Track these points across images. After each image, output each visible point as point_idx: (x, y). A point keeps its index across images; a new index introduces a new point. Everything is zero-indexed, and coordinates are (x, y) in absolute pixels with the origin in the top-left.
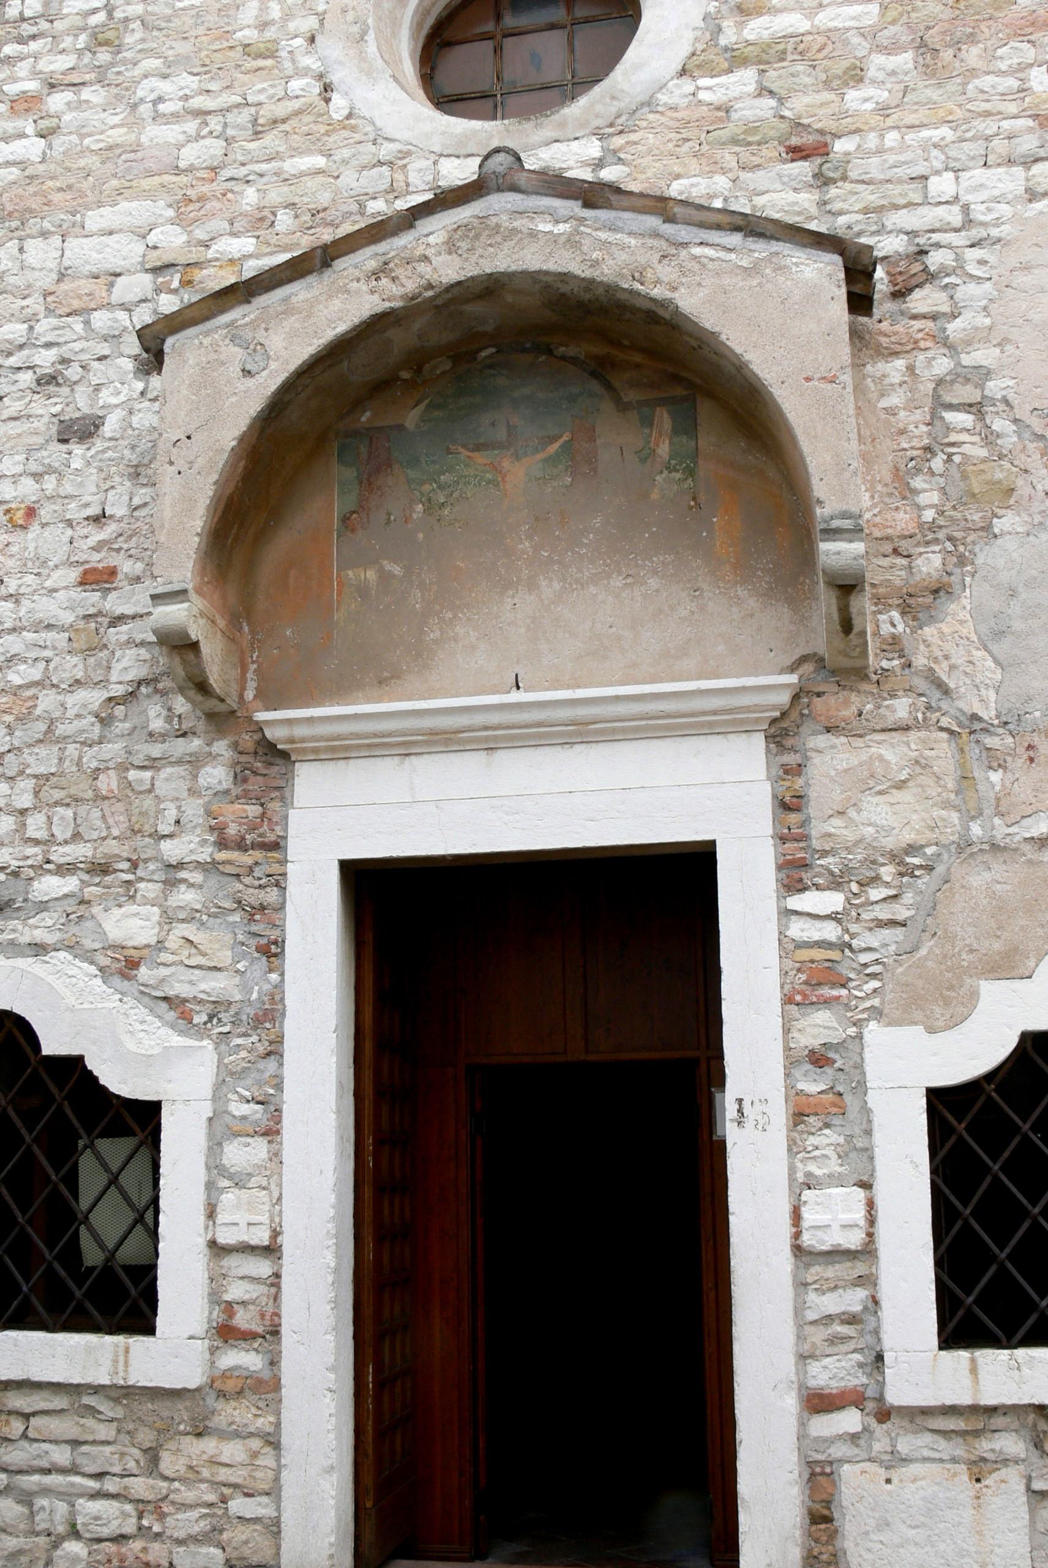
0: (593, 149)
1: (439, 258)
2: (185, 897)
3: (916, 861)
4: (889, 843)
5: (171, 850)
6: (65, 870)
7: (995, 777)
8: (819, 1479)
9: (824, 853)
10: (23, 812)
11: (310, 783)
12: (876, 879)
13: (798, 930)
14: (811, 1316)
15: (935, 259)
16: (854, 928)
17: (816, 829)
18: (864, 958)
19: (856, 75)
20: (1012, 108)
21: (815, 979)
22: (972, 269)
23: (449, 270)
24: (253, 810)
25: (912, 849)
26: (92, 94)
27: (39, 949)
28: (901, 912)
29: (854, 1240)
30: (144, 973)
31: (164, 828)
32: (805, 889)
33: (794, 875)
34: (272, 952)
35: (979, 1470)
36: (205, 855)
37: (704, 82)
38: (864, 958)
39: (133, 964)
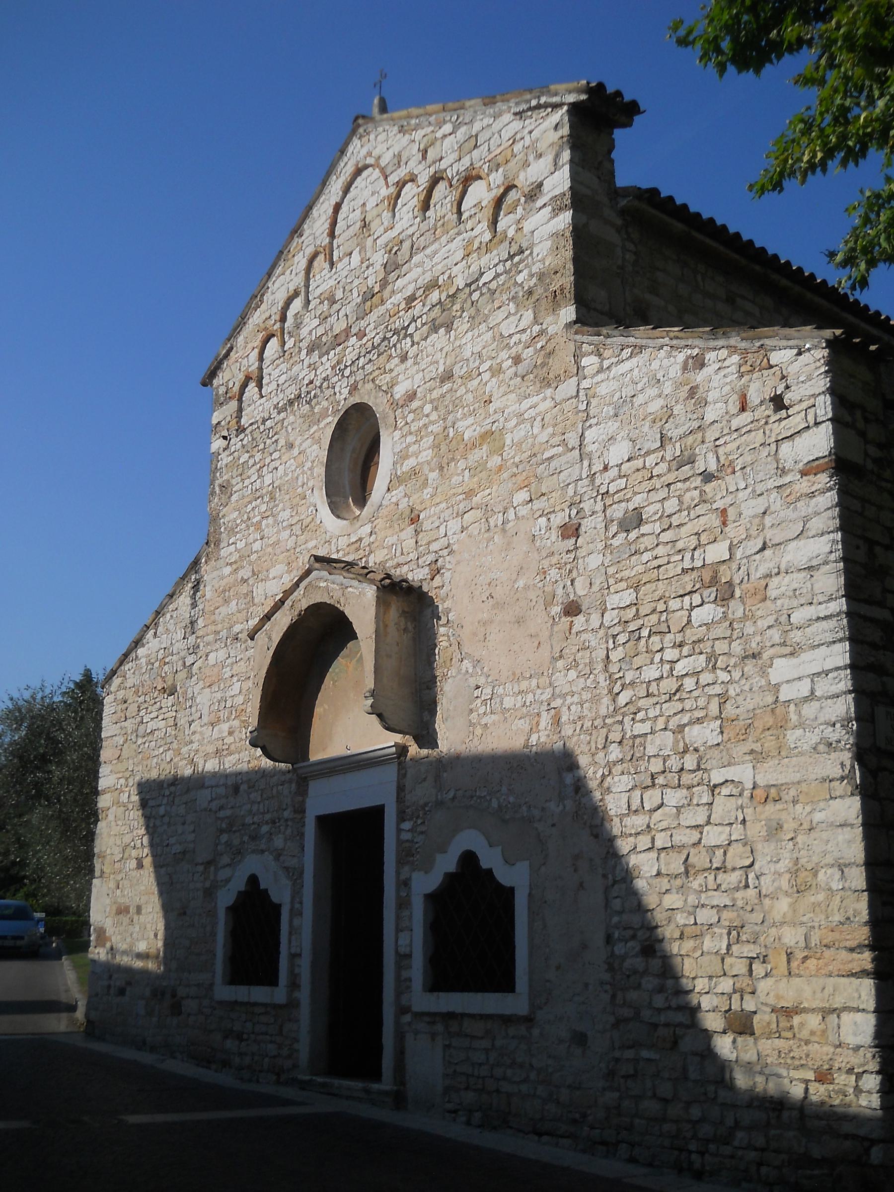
0: (367, 529)
1: (302, 600)
2: (289, 831)
3: (427, 809)
4: (421, 802)
5: (286, 814)
6: (267, 823)
7: (445, 775)
8: (400, 1037)
9: (408, 807)
10: (259, 803)
11: (315, 787)
12: (418, 817)
13: (405, 836)
14: (403, 978)
15: (439, 563)
16: (415, 835)
17: (408, 797)
18: (417, 846)
19: (425, 484)
20: (460, 490)
21: (406, 855)
22: (448, 566)
23: (304, 604)
24: (301, 798)
25: (426, 804)
26: (270, 520)
27: (263, 852)
28: (423, 828)
29: (407, 951)
30: (281, 858)
31: (284, 807)
32: (405, 821)
33: (402, 816)
34: (303, 848)
35: (433, 1036)
36: (291, 817)
37: (394, 492)
38: (417, 846)
39: (280, 855)
